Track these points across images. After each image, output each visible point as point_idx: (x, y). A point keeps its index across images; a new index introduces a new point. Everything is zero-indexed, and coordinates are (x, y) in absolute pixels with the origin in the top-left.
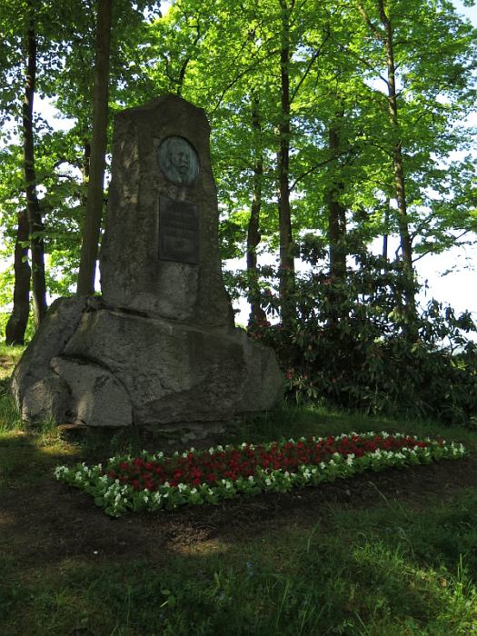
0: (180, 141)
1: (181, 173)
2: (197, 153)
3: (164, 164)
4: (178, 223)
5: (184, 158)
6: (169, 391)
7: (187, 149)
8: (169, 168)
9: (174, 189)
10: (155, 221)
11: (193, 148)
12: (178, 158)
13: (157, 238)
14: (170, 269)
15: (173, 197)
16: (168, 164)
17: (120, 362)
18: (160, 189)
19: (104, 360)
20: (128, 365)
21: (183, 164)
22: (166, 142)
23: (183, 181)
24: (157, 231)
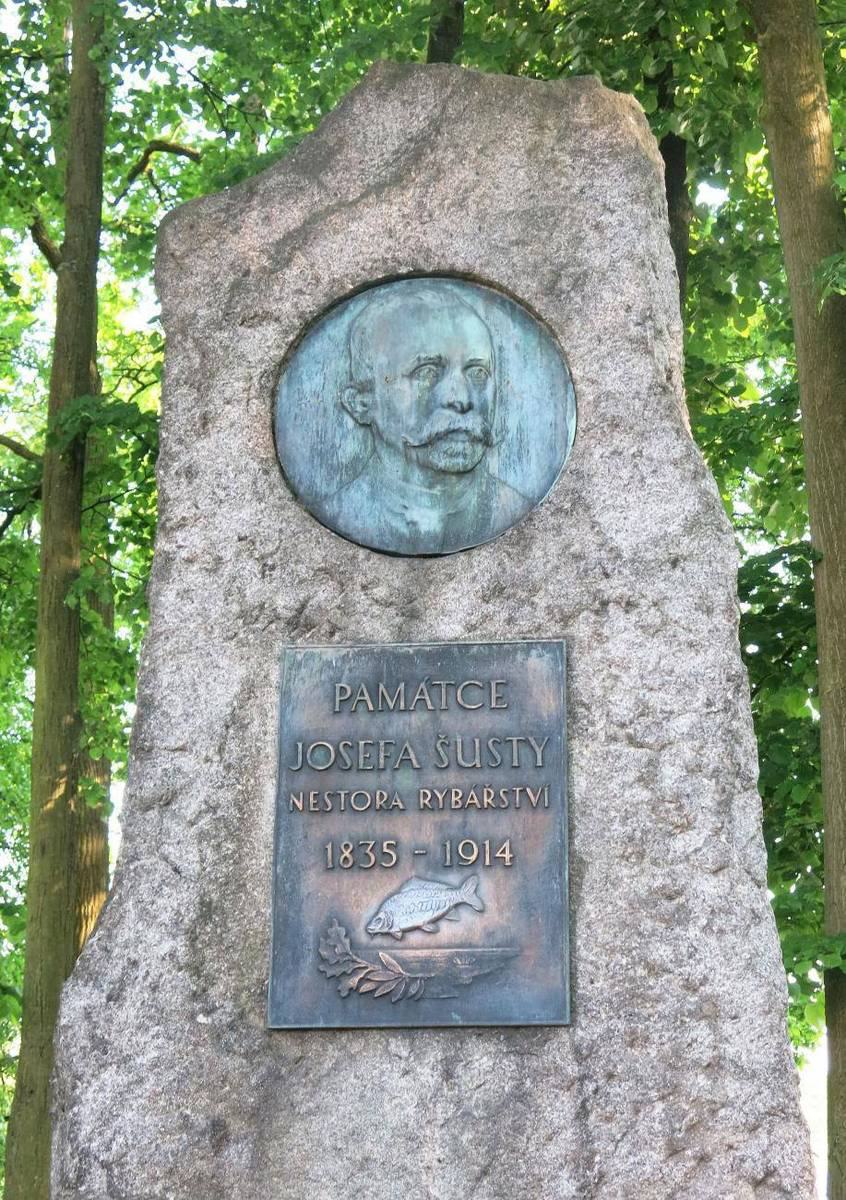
0: (429, 297)
1: (438, 475)
2: (544, 331)
3: (323, 453)
4: (405, 780)
5: (453, 386)
8: (355, 469)
9: (392, 576)
10: (245, 802)
11: (523, 312)
13: (261, 894)
14: (349, 1081)
15: (378, 629)
16: (351, 445)
18: (284, 602)
21: (442, 421)
22: (337, 329)
23: (450, 519)
24: (260, 860)
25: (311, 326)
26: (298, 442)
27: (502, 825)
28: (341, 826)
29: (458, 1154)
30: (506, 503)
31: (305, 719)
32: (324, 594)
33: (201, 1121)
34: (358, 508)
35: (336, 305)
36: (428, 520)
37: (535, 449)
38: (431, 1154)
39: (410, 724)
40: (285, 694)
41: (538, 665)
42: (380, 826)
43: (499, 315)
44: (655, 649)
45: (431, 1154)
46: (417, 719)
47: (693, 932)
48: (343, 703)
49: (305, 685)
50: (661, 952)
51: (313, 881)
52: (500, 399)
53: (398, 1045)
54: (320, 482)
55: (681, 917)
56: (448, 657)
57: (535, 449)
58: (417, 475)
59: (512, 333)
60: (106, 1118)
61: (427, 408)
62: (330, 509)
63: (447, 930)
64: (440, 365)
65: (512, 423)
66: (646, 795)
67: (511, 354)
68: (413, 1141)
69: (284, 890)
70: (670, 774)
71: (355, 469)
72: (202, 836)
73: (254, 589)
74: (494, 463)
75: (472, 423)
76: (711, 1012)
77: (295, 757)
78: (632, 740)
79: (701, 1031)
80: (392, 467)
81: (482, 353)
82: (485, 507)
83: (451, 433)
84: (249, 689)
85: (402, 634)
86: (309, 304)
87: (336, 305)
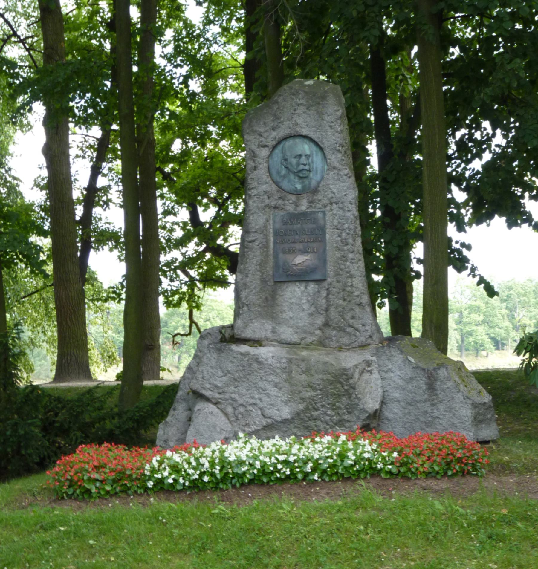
3: (278, 173)
5: (303, 160)
6: (269, 421)
7: (306, 148)
8: (284, 177)
9: (293, 198)
10: (267, 241)
12: (294, 161)
15: (290, 208)
16: (284, 172)
17: (220, 393)
19: (204, 392)
20: (227, 396)
21: (302, 167)
22: (280, 147)
24: (271, 252)
25: (274, 147)
26: (274, 172)
27: (315, 245)
28: (286, 246)
29: (308, 301)
30: (314, 183)
31: (278, 226)
32: (280, 202)
33: (264, 297)
34: (285, 185)
35: (279, 143)
36: (299, 187)
37: (319, 172)
38: (304, 301)
39: (297, 227)
40: (274, 221)
41: (320, 215)
42: (293, 245)
43: (312, 144)
44: (341, 212)
45: (304, 301)
46: (299, 226)
47: (348, 263)
48: (285, 223)
49: (278, 219)
50: (343, 267)
51: (281, 256)
52: (312, 162)
53: (298, 284)
54: (278, 179)
55: (346, 261)
56: (304, 214)
57: (319, 172)
58: (297, 178)
59: (314, 148)
60: (246, 297)
61: (298, 164)
62: (280, 185)
63: (305, 264)
64: (300, 156)
65: (314, 167)
66: (339, 239)
67: (314, 153)
68: (301, 299)
69: (276, 256)
70: (344, 235)
71: (284, 177)
72: (261, 248)
73: (267, 201)
74: (311, 175)
75: (307, 167)
76: (351, 276)
77: (276, 233)
78: (337, 229)
79: (349, 280)
80: (292, 176)
81: (308, 152)
82: (310, 184)
83: (303, 170)
84: (267, 221)
85: (295, 209)
86: (274, 143)
87: (279, 143)
